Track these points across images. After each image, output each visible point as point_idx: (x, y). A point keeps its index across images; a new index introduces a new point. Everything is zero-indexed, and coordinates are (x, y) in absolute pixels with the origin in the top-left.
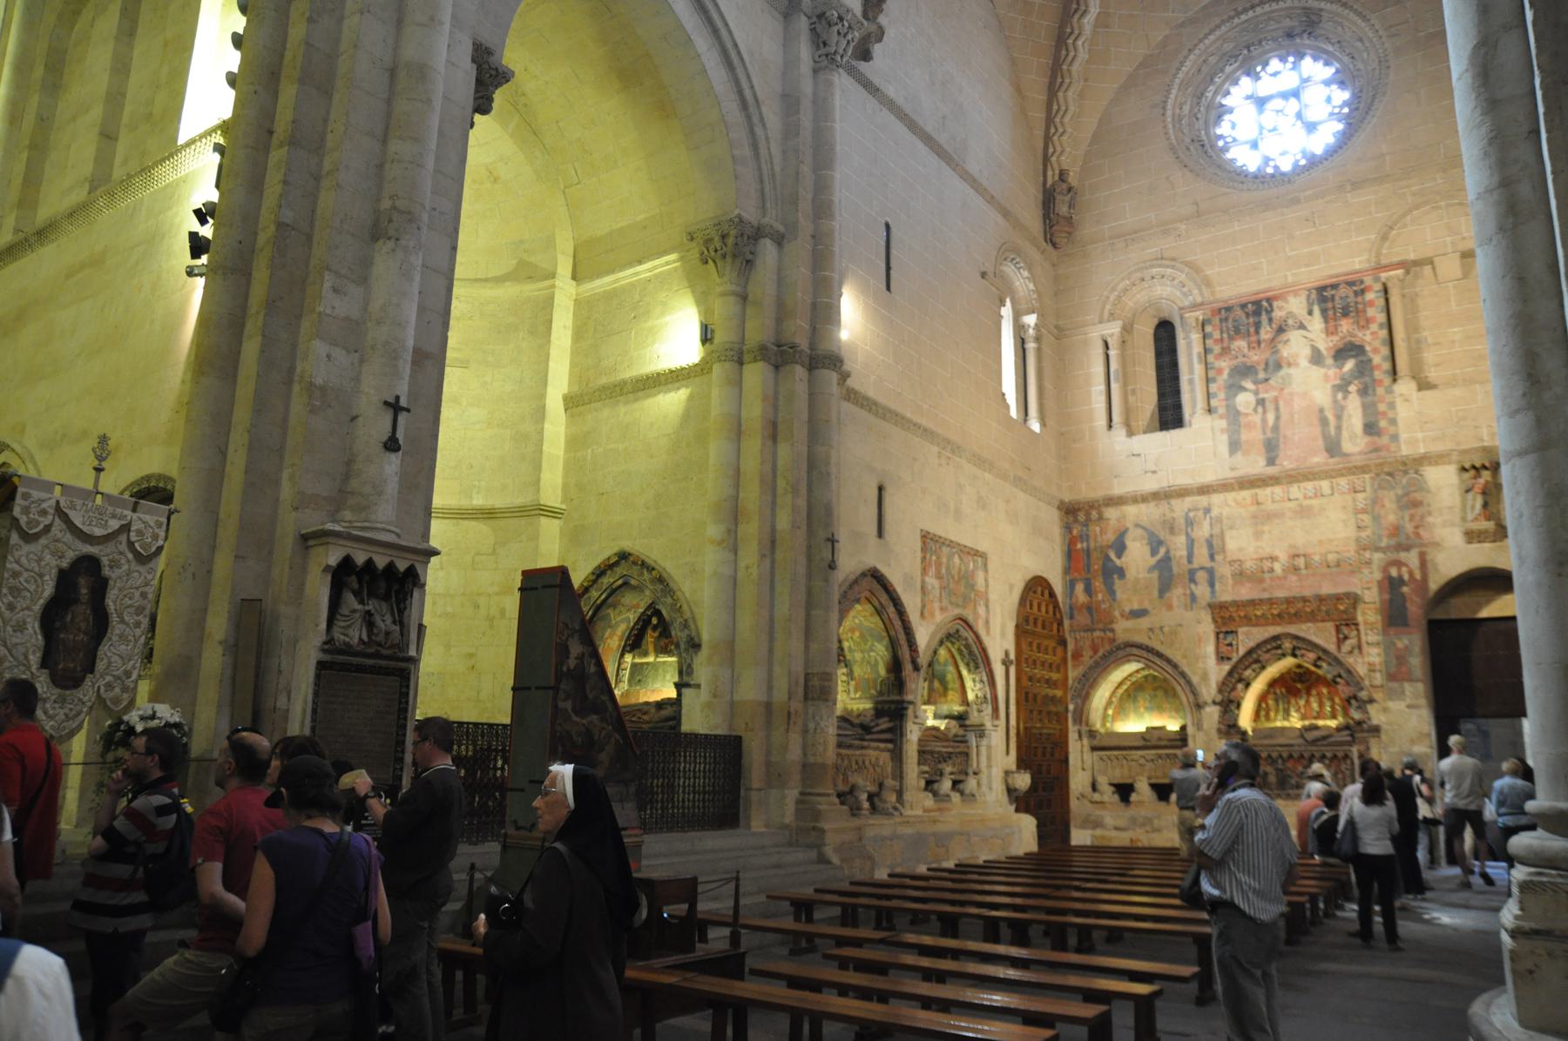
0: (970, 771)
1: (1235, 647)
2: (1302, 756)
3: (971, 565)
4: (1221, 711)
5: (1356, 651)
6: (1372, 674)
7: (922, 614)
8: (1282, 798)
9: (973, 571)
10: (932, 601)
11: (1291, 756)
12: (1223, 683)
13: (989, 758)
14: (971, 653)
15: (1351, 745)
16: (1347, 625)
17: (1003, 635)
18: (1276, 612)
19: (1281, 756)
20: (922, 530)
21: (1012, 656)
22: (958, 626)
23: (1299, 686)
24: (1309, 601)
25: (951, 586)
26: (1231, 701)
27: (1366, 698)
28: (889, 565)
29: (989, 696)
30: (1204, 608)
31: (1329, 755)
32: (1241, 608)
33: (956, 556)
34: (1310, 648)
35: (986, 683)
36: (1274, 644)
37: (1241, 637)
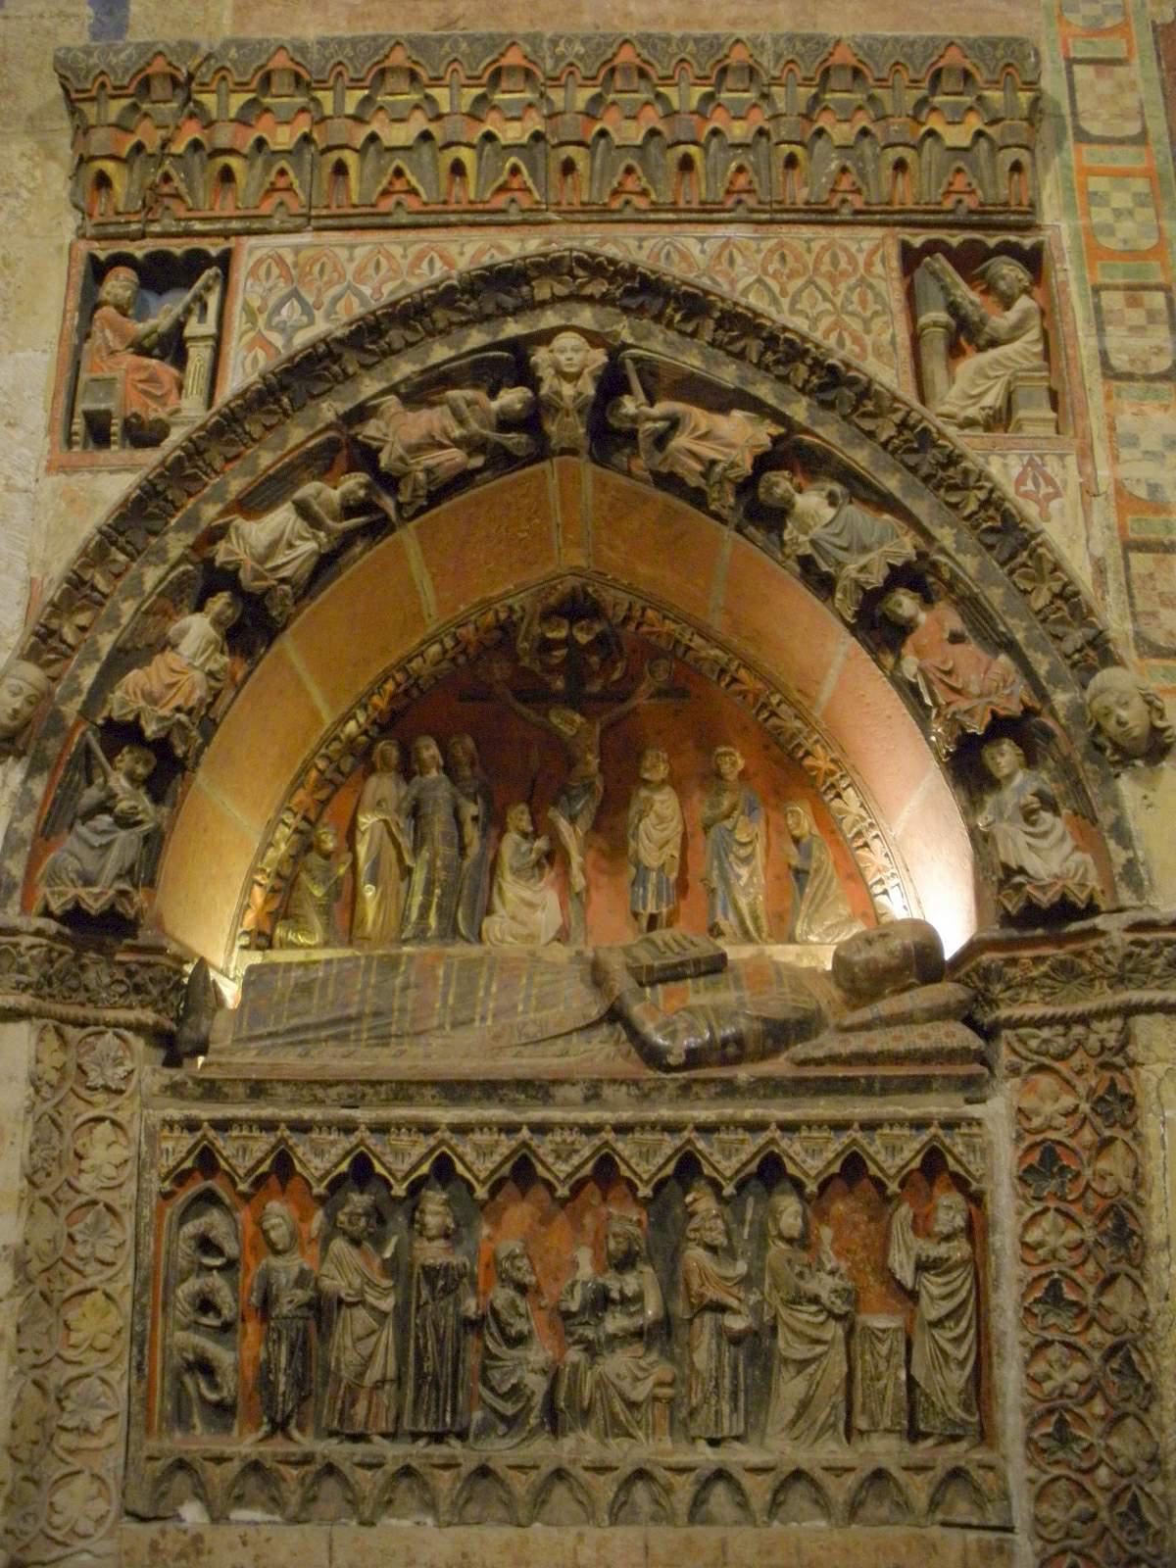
1: (198, 356)
2: (606, 1171)
4: (23, 803)
5: (1035, 414)
6: (1140, 562)
8: (431, 1506)
11: (522, 1172)
12: (77, 591)
15: (973, 1087)
16: (970, 262)
18: (513, 133)
19: (443, 1170)
23: (567, 723)
24: (752, 72)
26: (122, 734)
27: (1134, 718)
30: (33, 124)
31: (810, 1159)
32: (283, 99)
34: (728, 375)
36: (476, 338)
37: (247, 289)
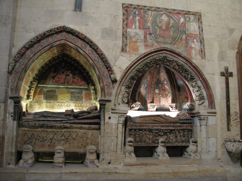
0: (191, 141)
3: (182, 20)
7: (123, 50)
9: (184, 25)
10: (136, 42)
13: (207, 133)
14: (186, 71)
17: (222, 57)
20: (123, 4)
21: (233, 69)
22: (164, 55)
25: (158, 33)
28: (88, 25)
29: (205, 94)
33: (164, 15)
35: (202, 87)
